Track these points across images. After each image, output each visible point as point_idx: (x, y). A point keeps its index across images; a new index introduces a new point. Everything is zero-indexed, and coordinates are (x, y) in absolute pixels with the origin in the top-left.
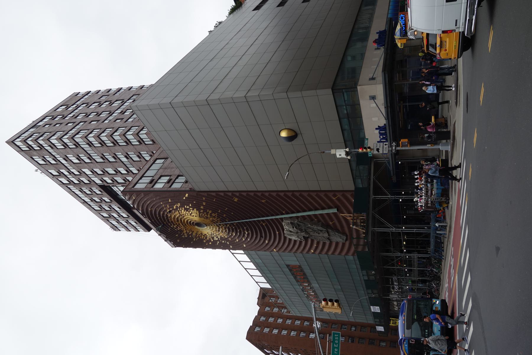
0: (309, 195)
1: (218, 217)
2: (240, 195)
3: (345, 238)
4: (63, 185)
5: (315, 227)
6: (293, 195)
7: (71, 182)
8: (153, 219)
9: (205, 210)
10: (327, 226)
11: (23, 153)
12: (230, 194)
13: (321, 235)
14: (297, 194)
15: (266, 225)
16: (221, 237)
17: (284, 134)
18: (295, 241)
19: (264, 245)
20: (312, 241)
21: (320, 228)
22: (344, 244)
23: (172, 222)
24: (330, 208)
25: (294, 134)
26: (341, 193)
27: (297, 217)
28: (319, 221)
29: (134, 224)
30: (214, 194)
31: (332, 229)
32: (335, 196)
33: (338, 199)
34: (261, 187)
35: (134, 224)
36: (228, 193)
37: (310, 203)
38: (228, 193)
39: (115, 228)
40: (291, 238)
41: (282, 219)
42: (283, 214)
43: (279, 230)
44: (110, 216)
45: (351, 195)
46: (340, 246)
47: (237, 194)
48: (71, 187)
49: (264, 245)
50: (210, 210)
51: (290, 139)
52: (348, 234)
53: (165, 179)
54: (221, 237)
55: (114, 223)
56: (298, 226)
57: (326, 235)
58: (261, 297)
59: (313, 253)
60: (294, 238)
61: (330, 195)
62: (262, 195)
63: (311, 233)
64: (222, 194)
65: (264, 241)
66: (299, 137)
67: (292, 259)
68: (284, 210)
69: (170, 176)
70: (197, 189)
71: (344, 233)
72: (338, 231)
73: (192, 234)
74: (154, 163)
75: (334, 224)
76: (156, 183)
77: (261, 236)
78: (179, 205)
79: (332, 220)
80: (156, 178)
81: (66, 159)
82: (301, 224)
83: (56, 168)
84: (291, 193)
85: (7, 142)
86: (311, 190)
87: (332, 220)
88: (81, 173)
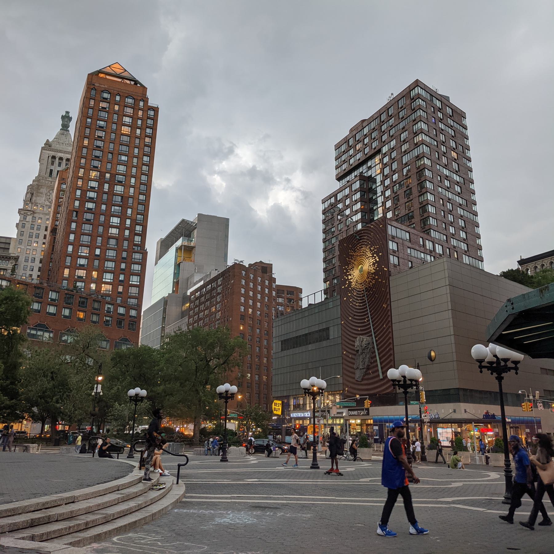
1: (370, 287)
4: (379, 114)
7: (382, 123)
8: (364, 233)
9: (374, 278)
11: (408, 90)
12: (388, 303)
13: (361, 364)
15: (365, 322)
16: (352, 282)
17: (433, 354)
18: (354, 342)
19: (348, 316)
20: (355, 355)
21: (366, 364)
23: (362, 247)
25: (433, 359)
27: (374, 348)
29: (344, 167)
30: (388, 290)
35: (344, 167)
39: (338, 147)
41: (371, 335)
42: (375, 338)
43: (361, 330)
44: (350, 147)
46: (352, 375)
47: (389, 308)
48: (377, 121)
49: (348, 316)
50: (375, 282)
51: (430, 358)
53: (395, 248)
54: (352, 282)
55: (343, 148)
56: (366, 348)
58: (263, 265)
59: (343, 353)
60: (357, 343)
63: (361, 356)
64: (388, 297)
65: (350, 316)
66: (431, 362)
67: (334, 333)
68: (379, 339)
69: (398, 251)
70: (391, 278)
73: (352, 259)
74: (406, 232)
76: (393, 241)
77: (354, 315)
78: (378, 260)
80: (396, 240)
81: (404, 129)
83: (395, 115)
85: (417, 81)
88: (392, 137)
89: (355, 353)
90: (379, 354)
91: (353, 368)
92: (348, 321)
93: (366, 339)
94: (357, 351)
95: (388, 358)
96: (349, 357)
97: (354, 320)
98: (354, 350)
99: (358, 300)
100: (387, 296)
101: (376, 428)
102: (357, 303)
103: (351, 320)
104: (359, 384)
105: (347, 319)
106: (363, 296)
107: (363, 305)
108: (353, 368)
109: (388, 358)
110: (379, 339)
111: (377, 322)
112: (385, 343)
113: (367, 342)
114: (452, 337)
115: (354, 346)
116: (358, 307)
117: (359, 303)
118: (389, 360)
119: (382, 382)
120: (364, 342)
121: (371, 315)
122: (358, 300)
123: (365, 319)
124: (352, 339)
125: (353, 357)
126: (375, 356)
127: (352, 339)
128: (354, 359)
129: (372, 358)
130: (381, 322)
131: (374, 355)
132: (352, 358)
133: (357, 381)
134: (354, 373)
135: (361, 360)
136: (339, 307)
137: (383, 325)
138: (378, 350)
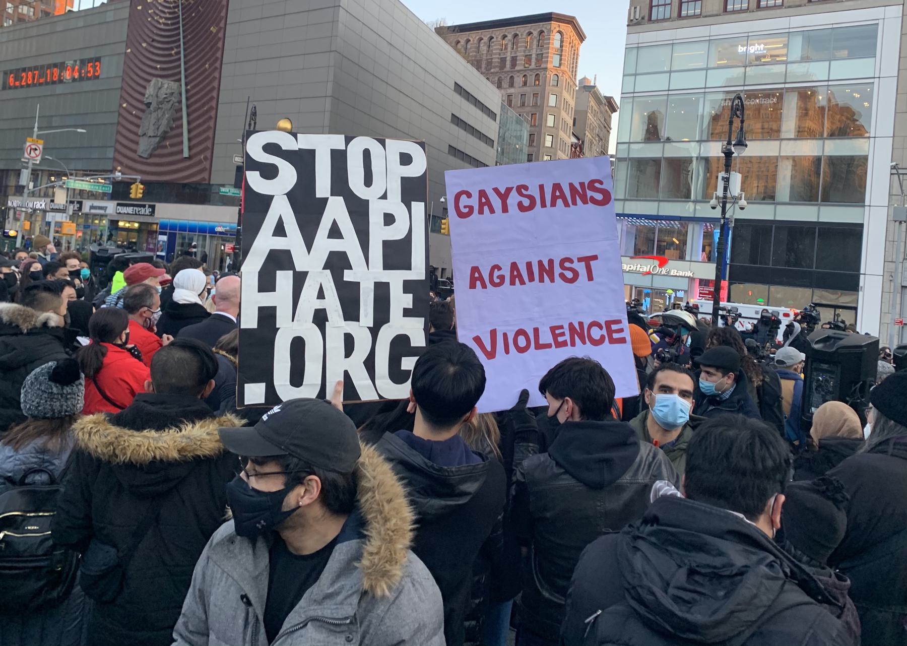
0: (209, 128)
2: (219, 39)
3: (145, 156)
5: (164, 122)
6: (211, 108)
10: (164, 137)
12: (222, 25)
13: (152, 127)
14: (213, 114)
15: (171, 55)
18: (145, 88)
19: (140, 40)
20: (143, 111)
22: (135, 152)
24: (190, 149)
26: (208, 167)
27: (180, 102)
28: (172, 129)
31: (159, 142)
32: (206, 158)
33: (200, 162)
36: (223, 22)
38: (223, 22)
40: (152, 83)
41: (179, 80)
42: (186, 85)
43: (162, 69)
45: (204, 179)
47: (221, 35)
49: (140, 40)
52: (149, 161)
56: (166, 100)
57: (151, 133)
59: (121, 105)
60: (150, 91)
61: (208, 154)
62: (216, 68)
63: (154, 115)
64: (223, 14)
65: (145, 41)
68: (193, 87)
71: (151, 156)
72: (154, 149)
75: (165, 147)
79: (172, 145)
82: (170, 105)
84: (214, 106)
87: (172, 145)
89: (144, 107)
90: (188, 115)
91: (136, 134)
92: (140, 49)
93: (168, 85)
94: (148, 105)
95: (204, 122)
96: (132, 114)
97: (152, 50)
98: (142, 102)
99: (164, 12)
100: (220, 12)
101: (164, 238)
102: (161, 17)
103: (146, 49)
104: (142, 163)
105: (137, 45)
106: (174, 7)
107: (172, 24)
108: (136, 134)
109: (204, 122)
110: (193, 87)
111: (195, 78)
112: (202, 97)
113: (169, 91)
114: (329, 100)
115: (143, 95)
116: (162, 27)
117: (166, 19)
118: (205, 127)
119: (187, 163)
120: (163, 91)
121: (184, 44)
122: (164, 12)
123: (172, 49)
124: (141, 82)
125: (140, 114)
126: (181, 118)
127: (141, 82)
128: (140, 118)
129: (174, 120)
130: (201, 59)
131: (178, 115)
132: (136, 116)
133: (140, 157)
134: (137, 143)
135: (153, 121)
136: (127, 22)
137: (205, 64)
138: (188, 107)
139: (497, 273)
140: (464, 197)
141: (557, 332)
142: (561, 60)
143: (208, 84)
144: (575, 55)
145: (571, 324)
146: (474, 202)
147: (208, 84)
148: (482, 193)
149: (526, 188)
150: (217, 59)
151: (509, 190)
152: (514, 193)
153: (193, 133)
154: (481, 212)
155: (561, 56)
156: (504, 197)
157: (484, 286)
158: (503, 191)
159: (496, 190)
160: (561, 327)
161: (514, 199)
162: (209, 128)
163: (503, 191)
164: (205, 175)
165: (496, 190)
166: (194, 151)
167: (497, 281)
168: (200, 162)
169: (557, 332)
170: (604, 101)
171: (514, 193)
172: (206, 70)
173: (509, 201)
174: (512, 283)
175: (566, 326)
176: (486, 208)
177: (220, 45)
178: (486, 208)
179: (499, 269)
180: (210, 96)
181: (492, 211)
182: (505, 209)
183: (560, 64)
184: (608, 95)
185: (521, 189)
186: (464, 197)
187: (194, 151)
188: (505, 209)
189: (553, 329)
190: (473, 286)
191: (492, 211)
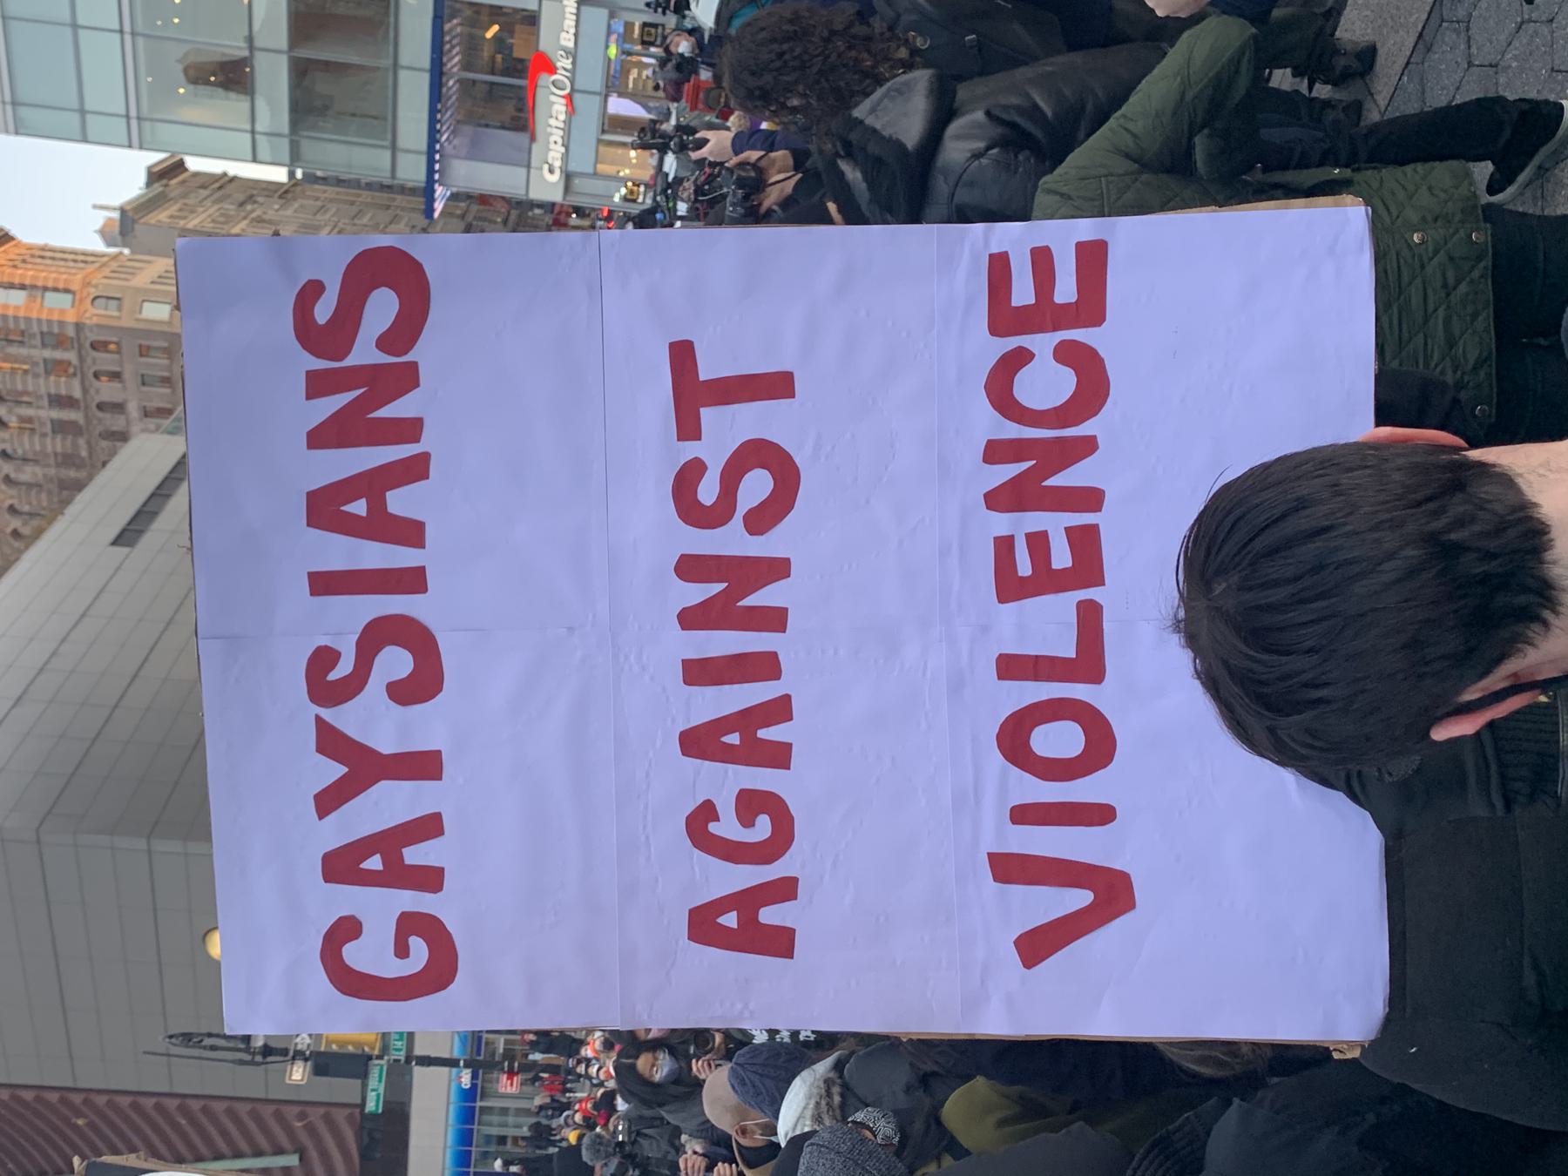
0: (230, 1113)
24: (279, 1151)
26: (322, 1110)
32: (302, 1116)
33: (311, 1129)
34: (91, 1077)
37: (224, 1133)
45: (350, 1118)
62: (86, 1101)
86: (238, 1095)
114: (159, 845)
137: (75, 1127)
139: (727, 827)
140: (356, 955)
141: (1024, 567)
142: (56, 290)
143: (126, 1119)
144: (45, 254)
145: (997, 500)
146: (378, 909)
147: (126, 1119)
148: (341, 866)
149: (323, 659)
150: (63, 1100)
151: (331, 741)
152: (348, 718)
153: (243, 1145)
154: (431, 879)
155: (45, 289)
156: (362, 767)
157: (785, 890)
158: (335, 771)
159: (328, 801)
160: (1004, 546)
161: (375, 721)
162: (230, 1113)
163: (335, 771)
164: (340, 1116)
165: (328, 801)
166: (284, 1141)
167: (763, 828)
168: (311, 1129)
169: (1024, 567)
170: (158, 188)
171: (348, 718)
172: (91, 1125)
173: (386, 745)
174: (779, 756)
175: (1003, 523)
176: (415, 855)
177: (28, 1096)
178: (415, 855)
179: (706, 811)
180: (154, 1114)
181: (430, 826)
182: (424, 766)
183: (67, 291)
184: (142, 179)
185: (326, 682)
186: (356, 955)
187: (284, 1141)
188: (424, 766)
189: (1010, 588)
190: (780, 943)
191: (430, 826)
